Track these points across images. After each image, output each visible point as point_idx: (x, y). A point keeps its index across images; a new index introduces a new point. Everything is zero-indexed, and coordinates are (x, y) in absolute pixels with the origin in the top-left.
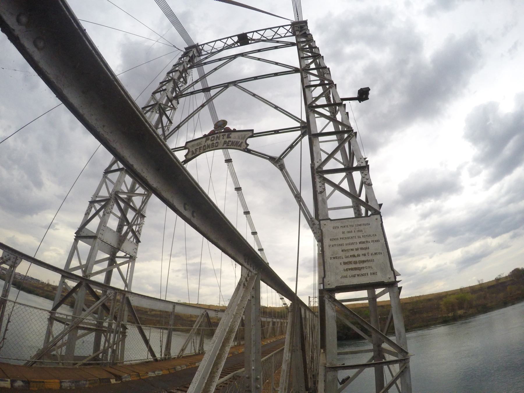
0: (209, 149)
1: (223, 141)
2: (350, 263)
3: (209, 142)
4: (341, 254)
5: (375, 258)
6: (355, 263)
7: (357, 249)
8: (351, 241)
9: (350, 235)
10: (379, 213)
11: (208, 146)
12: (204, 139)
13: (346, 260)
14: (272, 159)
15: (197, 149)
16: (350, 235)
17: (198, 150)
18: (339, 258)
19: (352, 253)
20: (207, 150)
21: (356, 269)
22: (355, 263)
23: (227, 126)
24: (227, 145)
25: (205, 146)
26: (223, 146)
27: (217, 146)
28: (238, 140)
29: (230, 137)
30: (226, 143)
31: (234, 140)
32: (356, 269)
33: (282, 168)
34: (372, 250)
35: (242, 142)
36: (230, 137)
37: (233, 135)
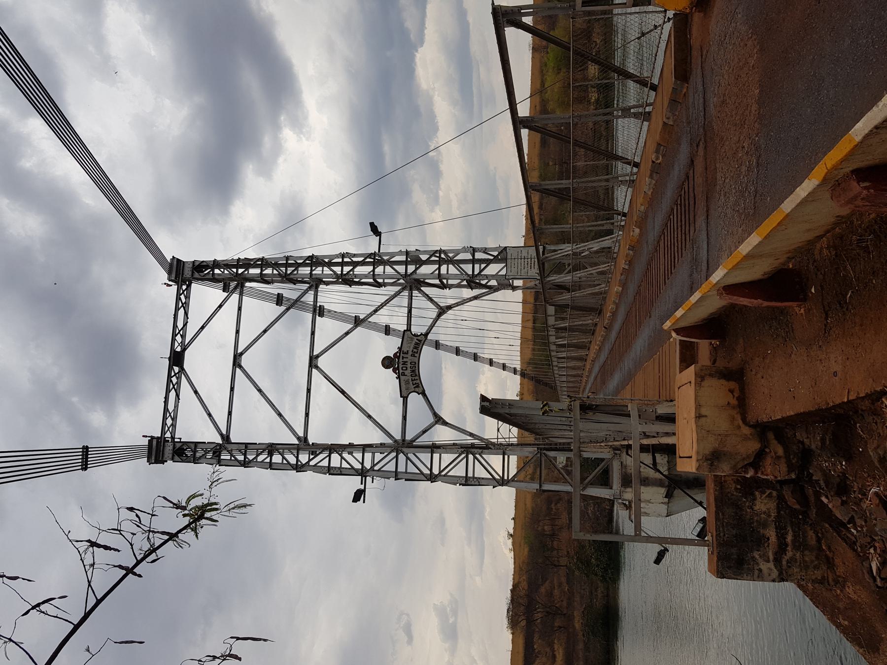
0: (417, 371)
1: (410, 357)
2: (531, 266)
3: (408, 372)
4: (526, 270)
5: (530, 254)
6: (531, 263)
7: (524, 262)
8: (520, 264)
9: (516, 265)
10: (506, 247)
11: (413, 371)
12: (402, 378)
13: (529, 268)
14: (439, 315)
15: (413, 383)
16: (516, 265)
17: (414, 382)
18: (528, 270)
19: (526, 265)
20: (417, 373)
21: (534, 264)
22: (531, 263)
23: (392, 356)
24: (417, 353)
25: (411, 376)
26: (416, 357)
27: (415, 363)
28: (414, 342)
29: (408, 351)
30: (414, 354)
31: (412, 347)
32: (534, 264)
33: (449, 307)
34: (526, 255)
35: (417, 339)
36: (408, 351)
37: (405, 349)
